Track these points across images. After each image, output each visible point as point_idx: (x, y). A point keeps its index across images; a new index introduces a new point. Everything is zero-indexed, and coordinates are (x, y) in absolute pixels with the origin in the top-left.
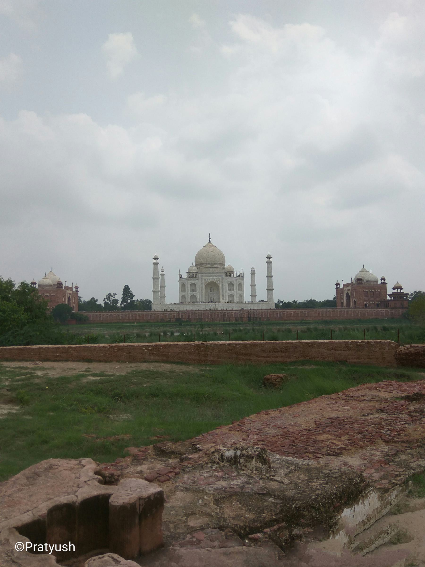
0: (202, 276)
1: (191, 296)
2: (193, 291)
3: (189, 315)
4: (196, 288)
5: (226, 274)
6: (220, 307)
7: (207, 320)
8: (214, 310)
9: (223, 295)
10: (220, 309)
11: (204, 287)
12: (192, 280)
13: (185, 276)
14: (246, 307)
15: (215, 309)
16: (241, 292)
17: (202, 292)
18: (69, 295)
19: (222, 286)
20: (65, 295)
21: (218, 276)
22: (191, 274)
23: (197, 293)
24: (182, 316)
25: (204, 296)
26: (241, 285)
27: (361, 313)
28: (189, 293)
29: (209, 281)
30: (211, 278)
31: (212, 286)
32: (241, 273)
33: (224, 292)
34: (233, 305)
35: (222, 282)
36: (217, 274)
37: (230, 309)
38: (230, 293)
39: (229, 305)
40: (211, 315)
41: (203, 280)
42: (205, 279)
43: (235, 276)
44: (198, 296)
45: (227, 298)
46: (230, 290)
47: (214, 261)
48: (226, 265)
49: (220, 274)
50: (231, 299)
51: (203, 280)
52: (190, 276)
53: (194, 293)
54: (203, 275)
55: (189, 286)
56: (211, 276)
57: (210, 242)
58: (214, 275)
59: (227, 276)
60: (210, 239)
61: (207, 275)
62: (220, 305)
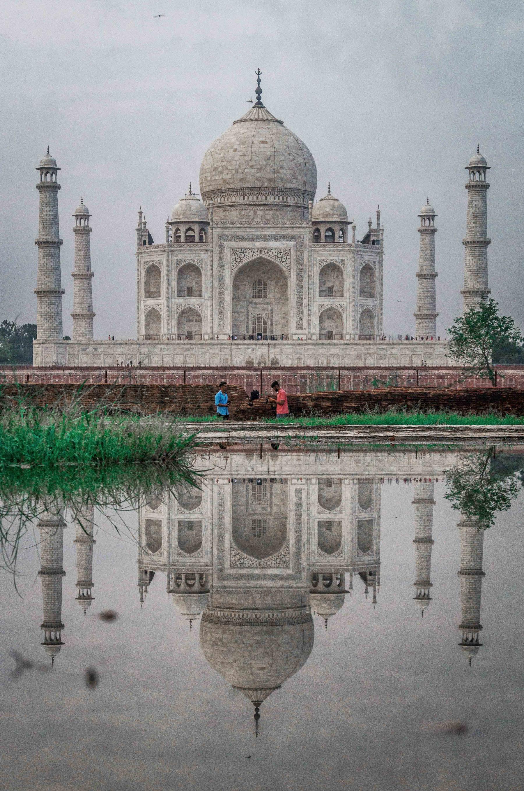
0: (222, 237)
1: (183, 312)
2: (190, 292)
4: (199, 283)
5: (318, 230)
6: (286, 356)
9: (300, 312)
10: (285, 361)
11: (228, 281)
12: (187, 255)
13: (160, 237)
14: (381, 358)
15: (268, 364)
16: (367, 302)
17: (221, 300)
19: (300, 276)
21: (284, 238)
22: (183, 229)
23: (204, 304)
25: (229, 314)
26: (372, 274)
28: (176, 301)
29: (249, 257)
30: (258, 244)
32: (374, 226)
33: (305, 302)
34: (335, 350)
35: (299, 262)
37: (323, 362)
38: (327, 302)
39: (322, 350)
41: (227, 252)
42: (233, 250)
43: (350, 240)
44: (207, 312)
45: (315, 321)
46: (329, 292)
47: (270, 180)
48: (321, 193)
49: (290, 232)
50: (330, 326)
51: (227, 252)
52: (178, 238)
53: (193, 301)
54: (226, 232)
55: (174, 275)
56: (257, 238)
57: (259, 105)
59: (317, 239)
60: (259, 91)
61: (241, 232)
62: (289, 350)
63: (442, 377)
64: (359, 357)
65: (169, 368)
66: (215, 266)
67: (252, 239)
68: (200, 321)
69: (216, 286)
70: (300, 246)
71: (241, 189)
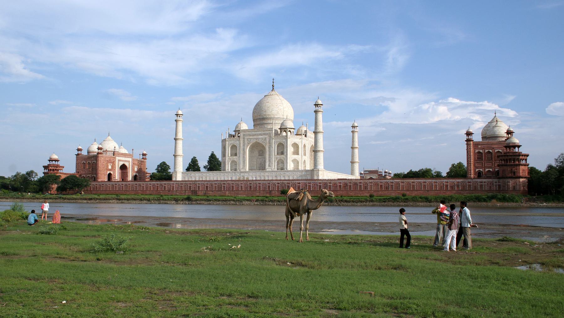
2: (236, 155)
3: (207, 187)
7: (227, 193)
8: (244, 181)
10: (250, 179)
16: (296, 157)
18: (121, 163)
19: (269, 148)
20: (113, 163)
21: (264, 134)
24: (199, 187)
27: (447, 186)
30: (255, 137)
31: (259, 150)
35: (270, 143)
36: (263, 132)
40: (233, 187)
46: (282, 153)
47: (269, 115)
50: (281, 165)
54: (245, 133)
56: (255, 135)
58: (260, 132)
60: (273, 86)
61: (250, 133)
63: (299, 183)
64: (276, 176)
65: (206, 181)
66: (242, 145)
67: (253, 135)
68: (236, 165)
69: (242, 152)
70: (270, 136)
71: (260, 119)
